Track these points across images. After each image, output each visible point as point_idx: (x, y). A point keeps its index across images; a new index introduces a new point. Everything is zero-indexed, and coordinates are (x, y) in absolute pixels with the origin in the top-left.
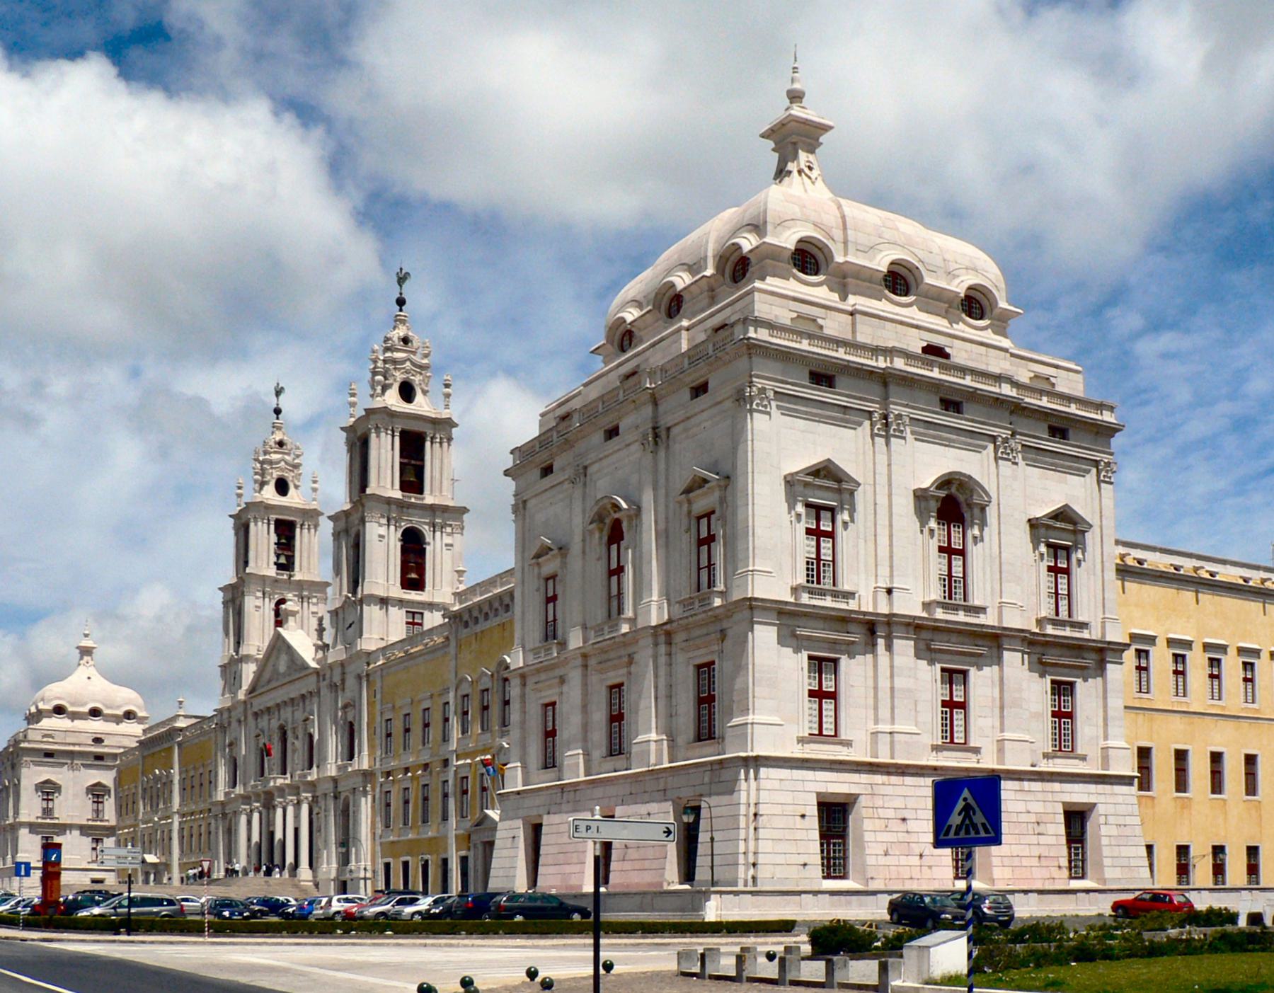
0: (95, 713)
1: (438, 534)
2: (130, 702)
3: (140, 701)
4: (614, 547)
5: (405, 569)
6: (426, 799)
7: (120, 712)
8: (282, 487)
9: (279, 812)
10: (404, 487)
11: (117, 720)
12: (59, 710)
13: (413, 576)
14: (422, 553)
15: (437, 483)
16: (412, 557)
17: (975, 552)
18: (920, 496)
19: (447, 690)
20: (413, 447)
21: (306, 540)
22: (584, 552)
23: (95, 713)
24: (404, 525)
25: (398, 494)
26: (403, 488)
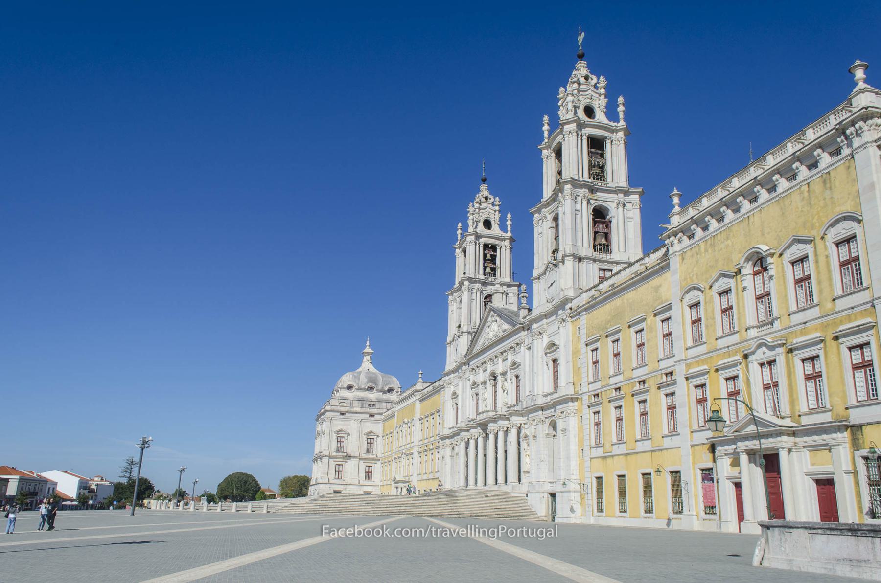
7: (386, 388)
11: (384, 392)
13: (604, 241)
14: (608, 224)
16: (601, 228)
19: (669, 307)
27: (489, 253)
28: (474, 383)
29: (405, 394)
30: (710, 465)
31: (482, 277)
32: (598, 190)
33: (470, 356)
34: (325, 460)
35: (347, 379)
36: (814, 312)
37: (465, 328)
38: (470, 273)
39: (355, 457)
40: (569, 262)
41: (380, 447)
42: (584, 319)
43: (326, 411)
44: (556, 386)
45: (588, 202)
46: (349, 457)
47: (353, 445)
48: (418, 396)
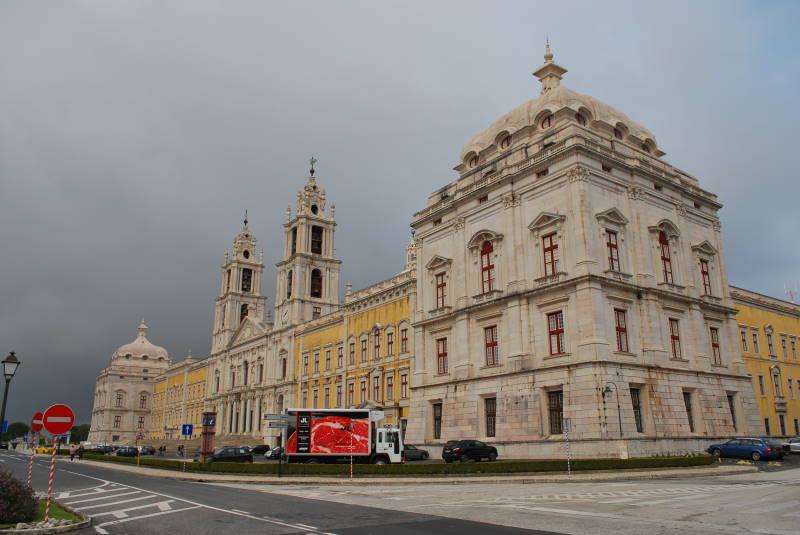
0: (145, 358)
5: (313, 286)
6: (327, 395)
8: (246, 254)
9: (243, 403)
10: (313, 251)
12: (128, 356)
14: (320, 280)
17: (674, 258)
18: (652, 230)
19: (342, 343)
20: (317, 232)
23: (145, 358)
24: (313, 268)
27: (247, 274)
28: (232, 366)
29: (176, 366)
31: (241, 292)
33: (230, 347)
35: (126, 349)
36: (392, 359)
37: (227, 327)
38: (233, 290)
39: (130, 411)
40: (297, 304)
41: (152, 404)
42: (301, 340)
44: (284, 375)
46: (126, 411)
47: (130, 402)
48: (187, 369)
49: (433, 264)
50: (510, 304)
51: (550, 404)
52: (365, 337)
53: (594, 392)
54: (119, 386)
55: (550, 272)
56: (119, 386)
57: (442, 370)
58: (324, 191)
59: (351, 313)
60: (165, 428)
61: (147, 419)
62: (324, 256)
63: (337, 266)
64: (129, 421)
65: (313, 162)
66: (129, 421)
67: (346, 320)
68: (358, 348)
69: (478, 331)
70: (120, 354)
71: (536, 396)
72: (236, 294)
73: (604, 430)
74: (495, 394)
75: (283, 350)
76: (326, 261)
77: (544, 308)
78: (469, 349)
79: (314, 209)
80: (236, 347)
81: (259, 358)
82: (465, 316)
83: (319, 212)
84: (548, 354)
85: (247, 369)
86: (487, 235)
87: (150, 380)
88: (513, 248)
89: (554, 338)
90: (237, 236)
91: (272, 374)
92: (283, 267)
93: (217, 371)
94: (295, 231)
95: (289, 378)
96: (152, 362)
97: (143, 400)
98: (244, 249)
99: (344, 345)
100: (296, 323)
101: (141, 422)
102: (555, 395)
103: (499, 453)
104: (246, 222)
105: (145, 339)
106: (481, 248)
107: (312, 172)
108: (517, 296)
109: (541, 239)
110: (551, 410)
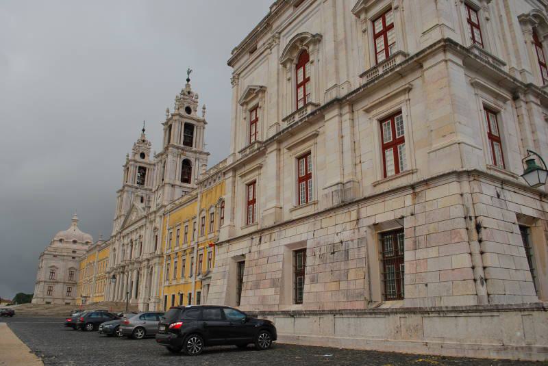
0: (75, 242)
1: (197, 162)
2: (89, 238)
3: (92, 239)
4: (301, 70)
5: (183, 174)
8: (143, 155)
10: (185, 143)
13: (186, 177)
14: (190, 169)
15: (197, 144)
19: (195, 217)
20: (189, 128)
21: (150, 174)
22: (278, 81)
23: (75, 242)
24: (183, 157)
25: (182, 146)
26: (184, 144)
27: (142, 171)
30: (199, 290)
32: (186, 151)
33: (123, 228)
34: (42, 284)
43: (44, 254)
45: (180, 157)
46: (57, 282)
49: (246, 97)
50: (327, 117)
51: (383, 253)
52: (213, 210)
53: (462, 223)
54: (53, 263)
55: (382, 57)
56: (53, 263)
57: (250, 218)
58: (197, 95)
59: (204, 189)
60: (82, 296)
61: (74, 289)
62: (194, 149)
63: (204, 156)
64: (59, 290)
65: (189, 72)
66: (59, 290)
67: (199, 196)
68: (207, 221)
69: (289, 161)
70: (55, 239)
71: (361, 240)
72: (131, 187)
73: (483, 291)
74: (304, 242)
75: (155, 228)
76: (195, 152)
77: (374, 112)
78: (278, 188)
79: (188, 110)
80: (129, 226)
81: (140, 236)
82: (275, 146)
83: (193, 113)
84: (379, 177)
85: (132, 246)
86: (302, 40)
87: (77, 259)
88: (333, 45)
89: (390, 154)
90: (136, 142)
91: (148, 248)
92: (159, 159)
93: (115, 249)
94: (170, 127)
95: (158, 252)
96: (80, 245)
97: (71, 275)
98: (141, 151)
99: (197, 220)
100: (166, 204)
101: (69, 291)
102: (391, 240)
103: (280, 332)
104: (144, 130)
105: (76, 228)
106: (295, 61)
107: (188, 80)
108: (338, 102)
109: (369, 23)
110: (385, 262)
